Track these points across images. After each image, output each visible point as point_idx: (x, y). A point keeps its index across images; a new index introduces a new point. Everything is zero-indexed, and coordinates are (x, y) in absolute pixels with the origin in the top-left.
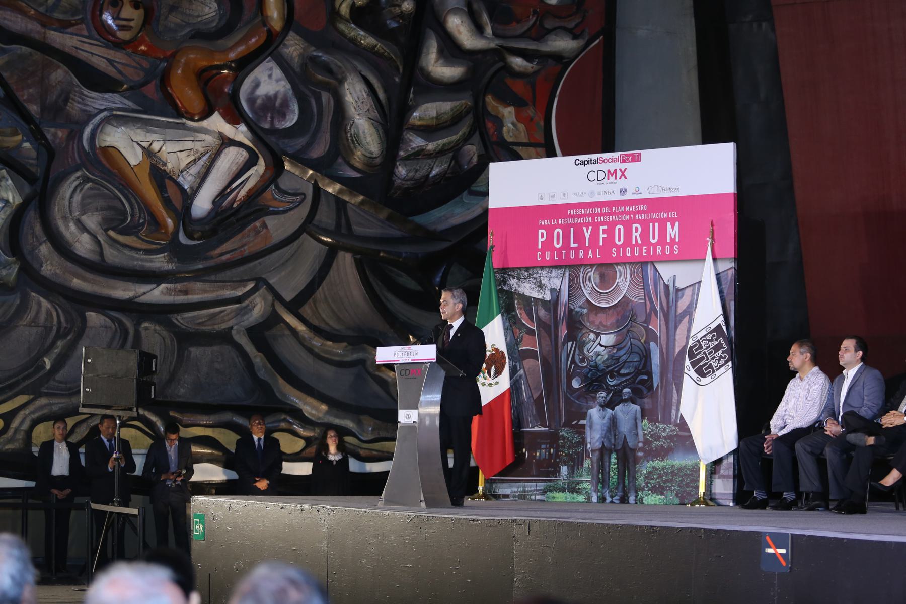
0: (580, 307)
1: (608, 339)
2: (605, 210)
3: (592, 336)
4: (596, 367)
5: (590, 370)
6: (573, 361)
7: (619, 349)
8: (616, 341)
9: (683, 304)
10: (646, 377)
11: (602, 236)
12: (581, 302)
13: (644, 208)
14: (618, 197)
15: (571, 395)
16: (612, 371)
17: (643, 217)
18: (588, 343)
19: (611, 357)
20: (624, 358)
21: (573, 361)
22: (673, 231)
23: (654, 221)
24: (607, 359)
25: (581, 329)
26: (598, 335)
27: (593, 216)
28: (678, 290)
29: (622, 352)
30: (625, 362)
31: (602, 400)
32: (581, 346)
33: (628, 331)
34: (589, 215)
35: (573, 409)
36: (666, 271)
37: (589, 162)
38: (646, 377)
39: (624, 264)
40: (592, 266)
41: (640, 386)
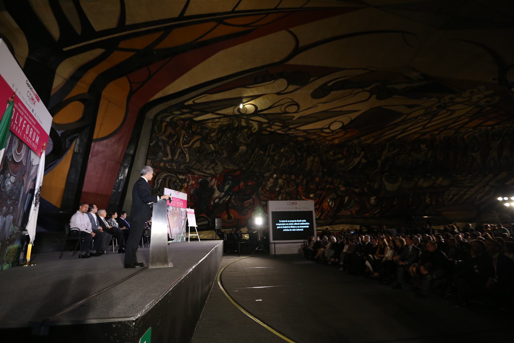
2: (27, 114)
3: (9, 175)
4: (6, 192)
7: (15, 186)
9: (33, 171)
11: (24, 126)
12: (10, 155)
13: (35, 123)
14: (31, 111)
17: (33, 126)
19: (12, 188)
22: (37, 140)
23: (36, 132)
27: (25, 114)
28: (33, 166)
31: (4, 212)
32: (5, 178)
34: (24, 112)
36: (33, 155)
37: (28, 84)
39: (26, 144)
40: (18, 138)
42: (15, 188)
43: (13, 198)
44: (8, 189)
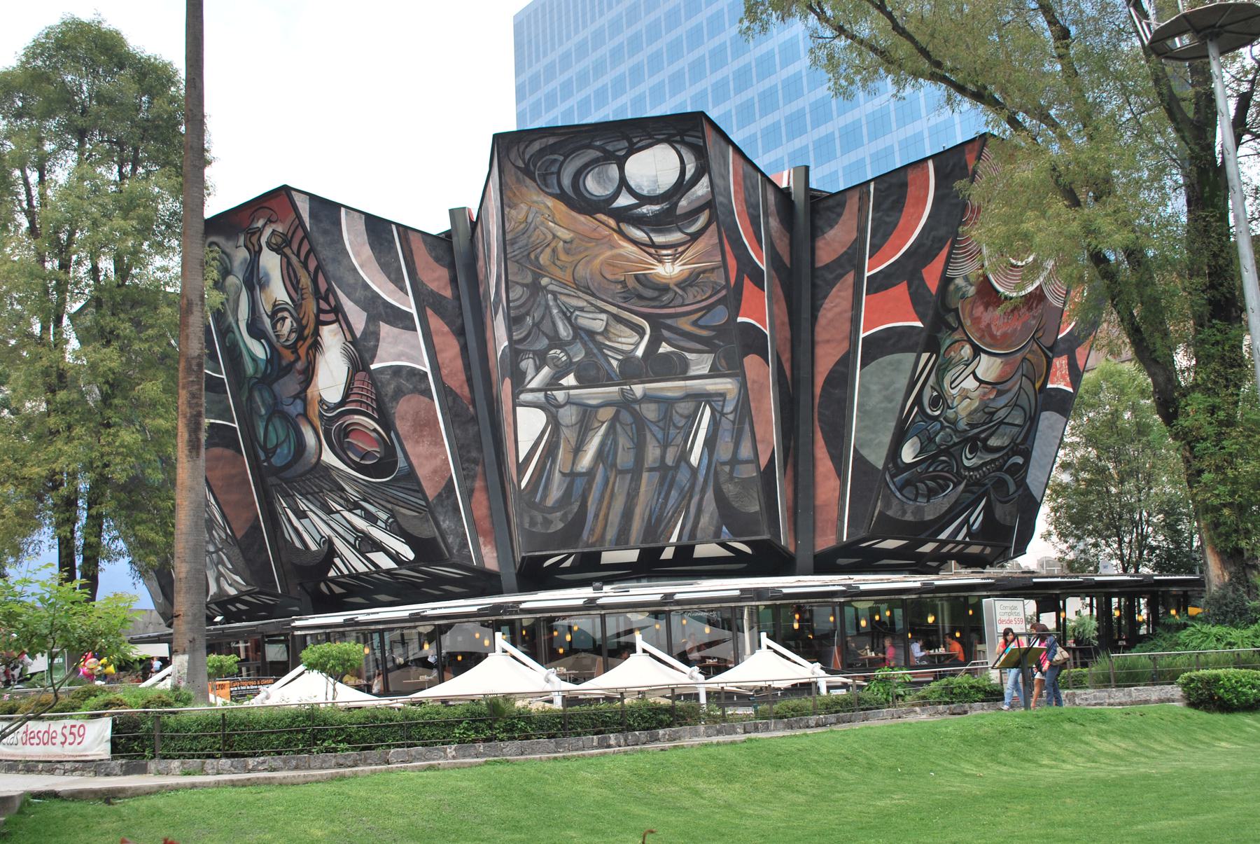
0: (966, 278)
1: (988, 367)
3: (967, 351)
5: (943, 428)
6: (918, 400)
7: (1000, 393)
8: (1000, 376)
10: (1020, 460)
15: (892, 477)
16: (976, 438)
18: (956, 365)
20: (1002, 414)
21: (918, 400)
24: (976, 411)
25: (954, 330)
26: (977, 351)
29: (1003, 400)
30: (1002, 423)
33: (1024, 359)
35: (889, 513)
38: (1020, 460)
41: (1008, 477)
42: (1003, 400)
43: (993, 442)
44: (963, 410)
